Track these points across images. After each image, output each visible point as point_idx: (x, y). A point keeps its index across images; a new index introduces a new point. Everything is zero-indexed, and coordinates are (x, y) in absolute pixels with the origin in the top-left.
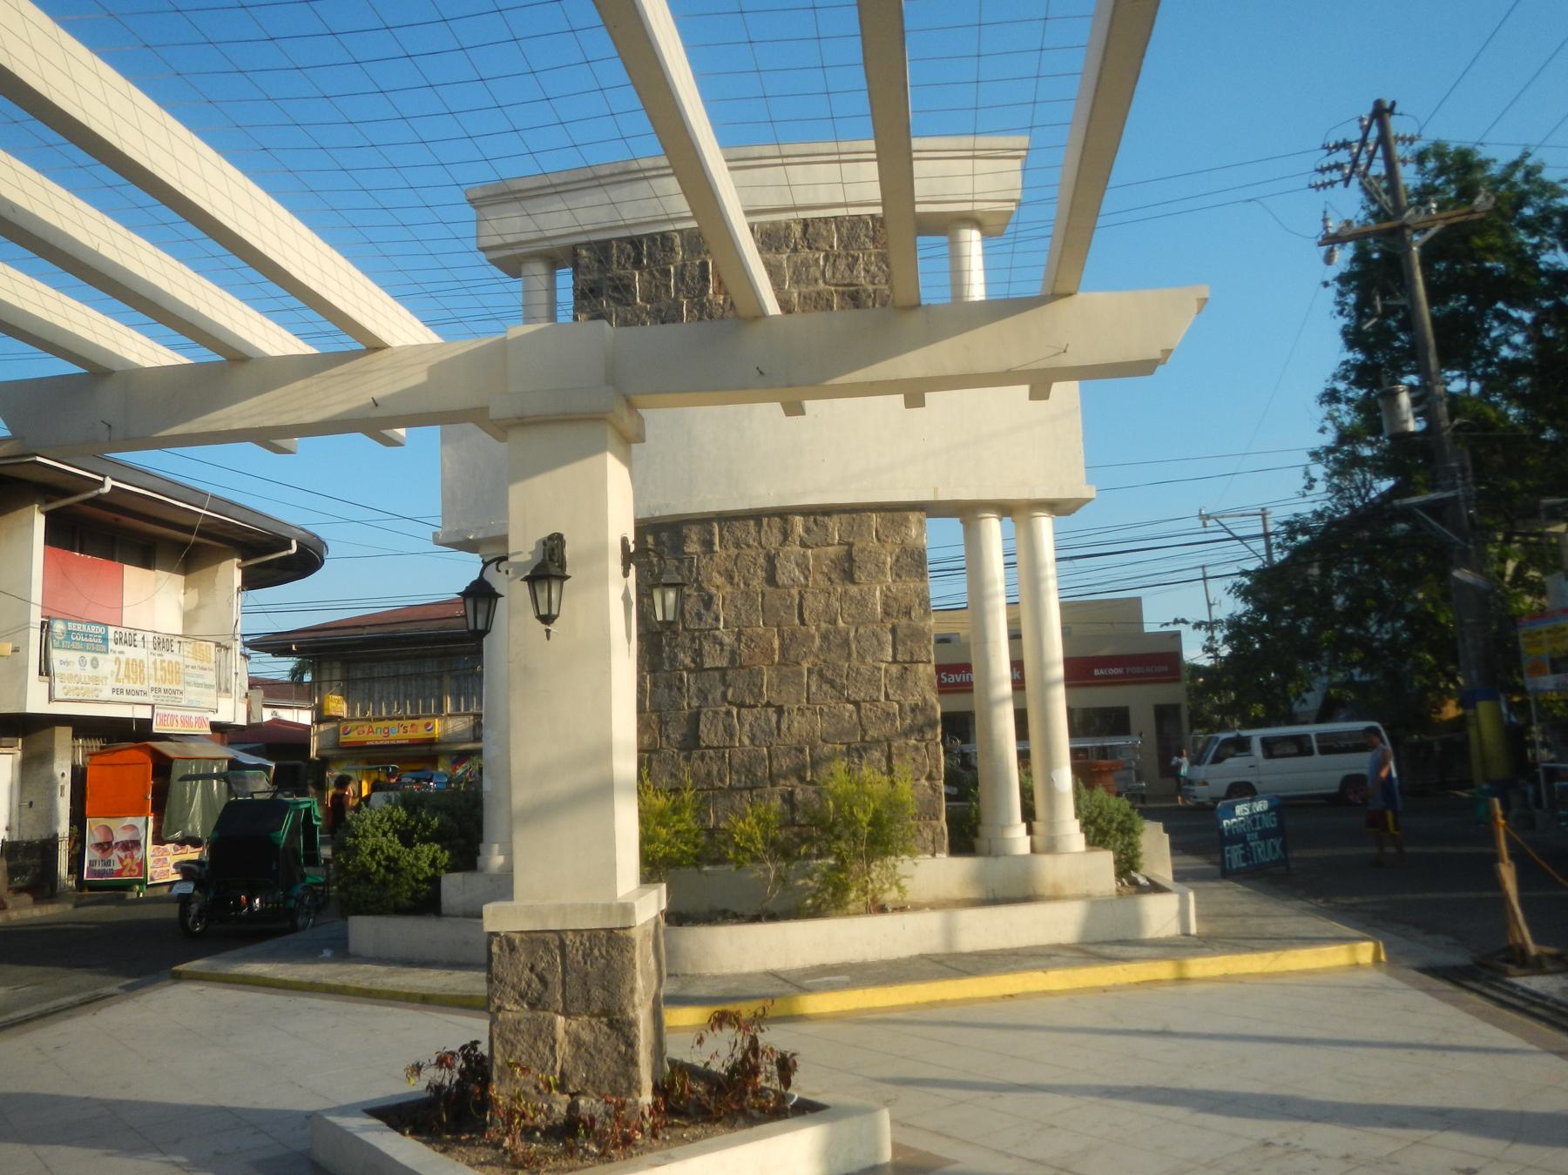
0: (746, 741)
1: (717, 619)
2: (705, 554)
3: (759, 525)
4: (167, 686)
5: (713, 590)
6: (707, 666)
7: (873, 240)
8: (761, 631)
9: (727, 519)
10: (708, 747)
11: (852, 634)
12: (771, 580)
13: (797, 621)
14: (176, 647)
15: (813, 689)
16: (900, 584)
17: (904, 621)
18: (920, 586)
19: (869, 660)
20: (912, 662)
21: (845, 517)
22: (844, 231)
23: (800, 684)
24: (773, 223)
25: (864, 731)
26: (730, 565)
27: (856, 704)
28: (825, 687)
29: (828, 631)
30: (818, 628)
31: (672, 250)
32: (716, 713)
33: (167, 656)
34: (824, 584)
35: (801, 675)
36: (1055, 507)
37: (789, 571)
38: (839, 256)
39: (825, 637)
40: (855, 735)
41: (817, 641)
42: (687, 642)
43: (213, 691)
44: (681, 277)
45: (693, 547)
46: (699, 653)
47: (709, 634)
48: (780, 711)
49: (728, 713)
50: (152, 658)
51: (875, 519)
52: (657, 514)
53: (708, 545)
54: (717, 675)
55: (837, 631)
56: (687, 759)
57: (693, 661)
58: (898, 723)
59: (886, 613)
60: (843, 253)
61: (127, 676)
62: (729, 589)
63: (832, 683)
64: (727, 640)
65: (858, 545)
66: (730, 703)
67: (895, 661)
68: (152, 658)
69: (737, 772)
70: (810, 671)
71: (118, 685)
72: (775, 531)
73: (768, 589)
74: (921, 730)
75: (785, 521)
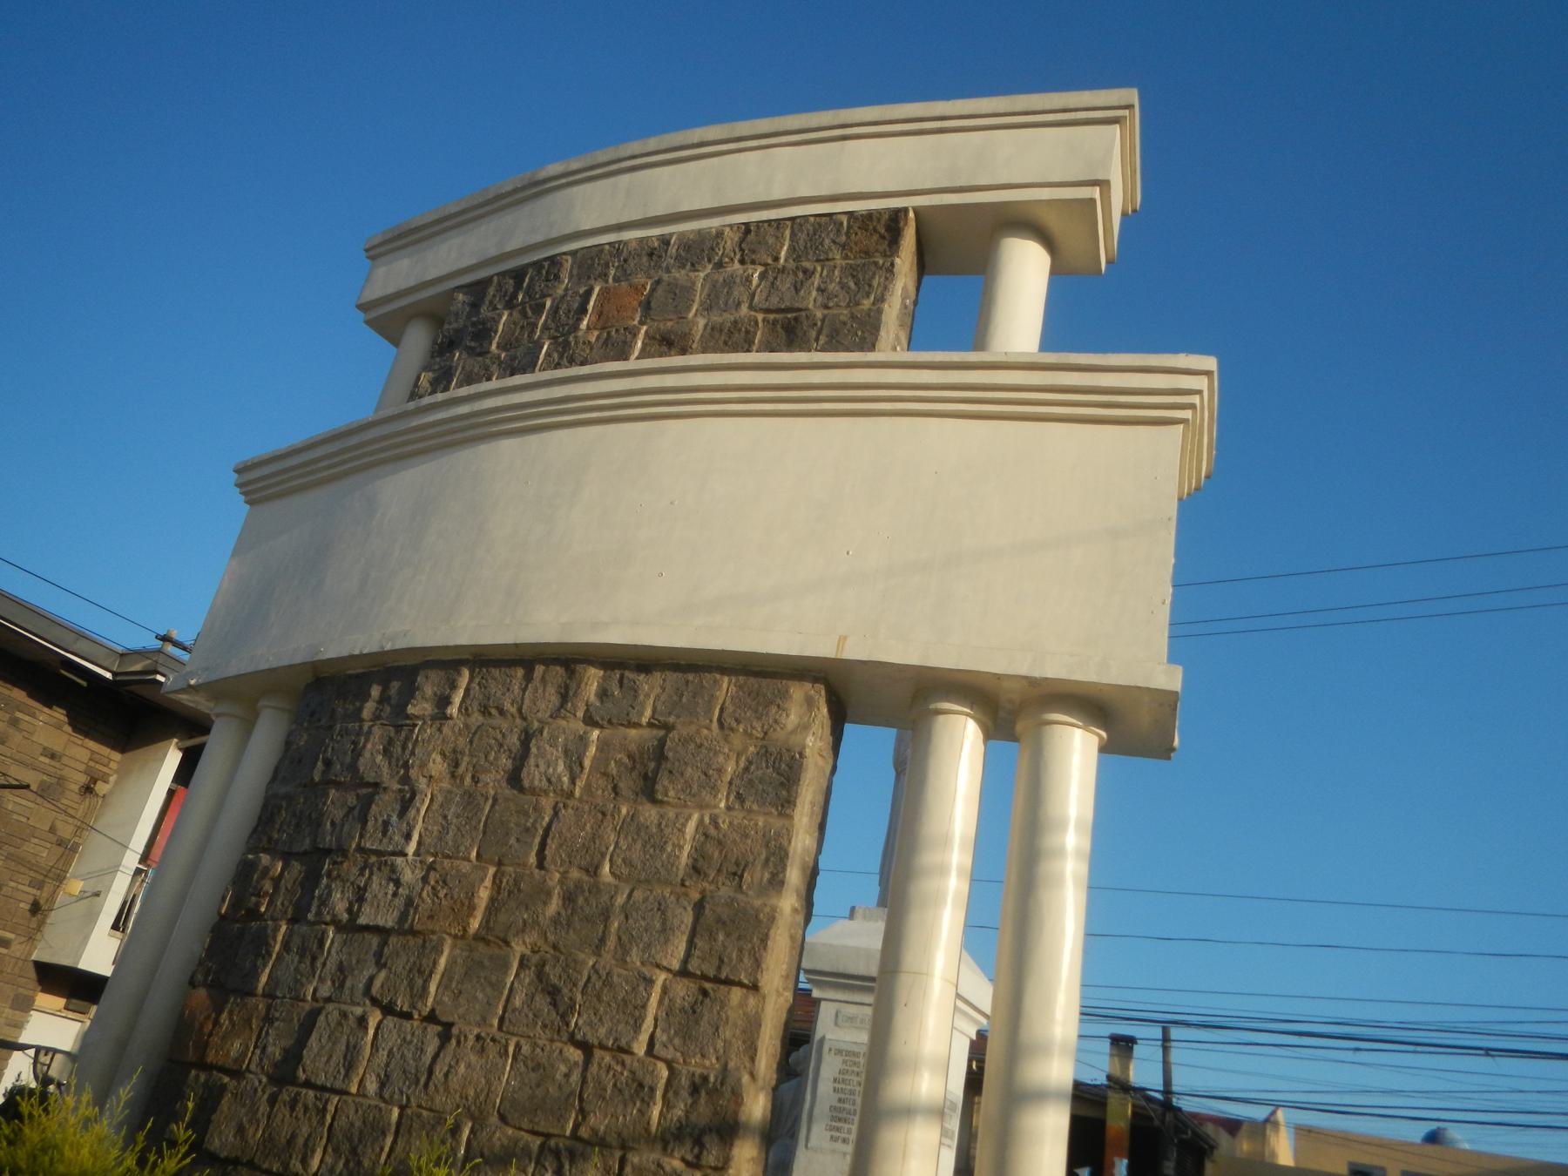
0: (372, 1086)
1: (408, 837)
2: (434, 718)
3: (528, 678)
5: (422, 783)
6: (362, 921)
7: (843, 246)
8: (465, 867)
9: (483, 660)
10: (308, 1084)
11: (620, 900)
12: (514, 779)
13: (532, 859)
15: (517, 1002)
16: (738, 816)
17: (725, 891)
18: (777, 823)
19: (635, 957)
20: (717, 980)
21: (673, 678)
22: (802, 237)
23: (497, 986)
24: (699, 231)
25: (583, 1112)
26: (462, 742)
27: (586, 1048)
28: (542, 1002)
29: (578, 886)
30: (564, 874)
31: (557, 277)
32: (344, 1015)
34: (602, 794)
35: (505, 966)
36: (1093, 705)
37: (547, 765)
38: (783, 270)
39: (569, 898)
40: (562, 1119)
41: (554, 906)
42: (355, 871)
44: (555, 310)
45: (420, 707)
46: (360, 895)
47: (384, 861)
48: (445, 1037)
49: (362, 1022)
51: (725, 687)
52: (388, 647)
53: (444, 701)
54: (375, 941)
55: (596, 889)
56: (272, 1100)
57: (349, 910)
58: (655, 1112)
59: (696, 869)
60: (792, 264)
62: (445, 785)
63: (553, 993)
64: (409, 876)
65: (682, 730)
66: (375, 1002)
67: (684, 972)
69: (336, 1150)
70: (523, 963)
72: (551, 690)
73: (508, 792)
74: (699, 1142)
75: (571, 673)
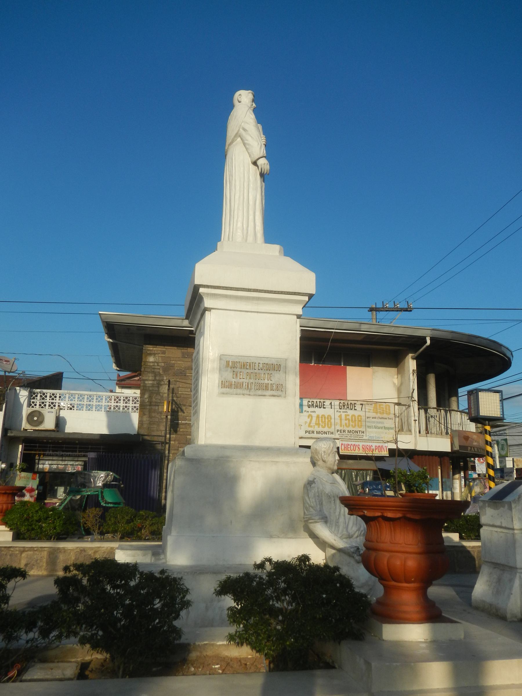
4: (351, 429)
14: (358, 407)
33: (350, 412)
43: (393, 432)
50: (338, 414)
61: (318, 424)
68: (338, 414)
71: (310, 429)
